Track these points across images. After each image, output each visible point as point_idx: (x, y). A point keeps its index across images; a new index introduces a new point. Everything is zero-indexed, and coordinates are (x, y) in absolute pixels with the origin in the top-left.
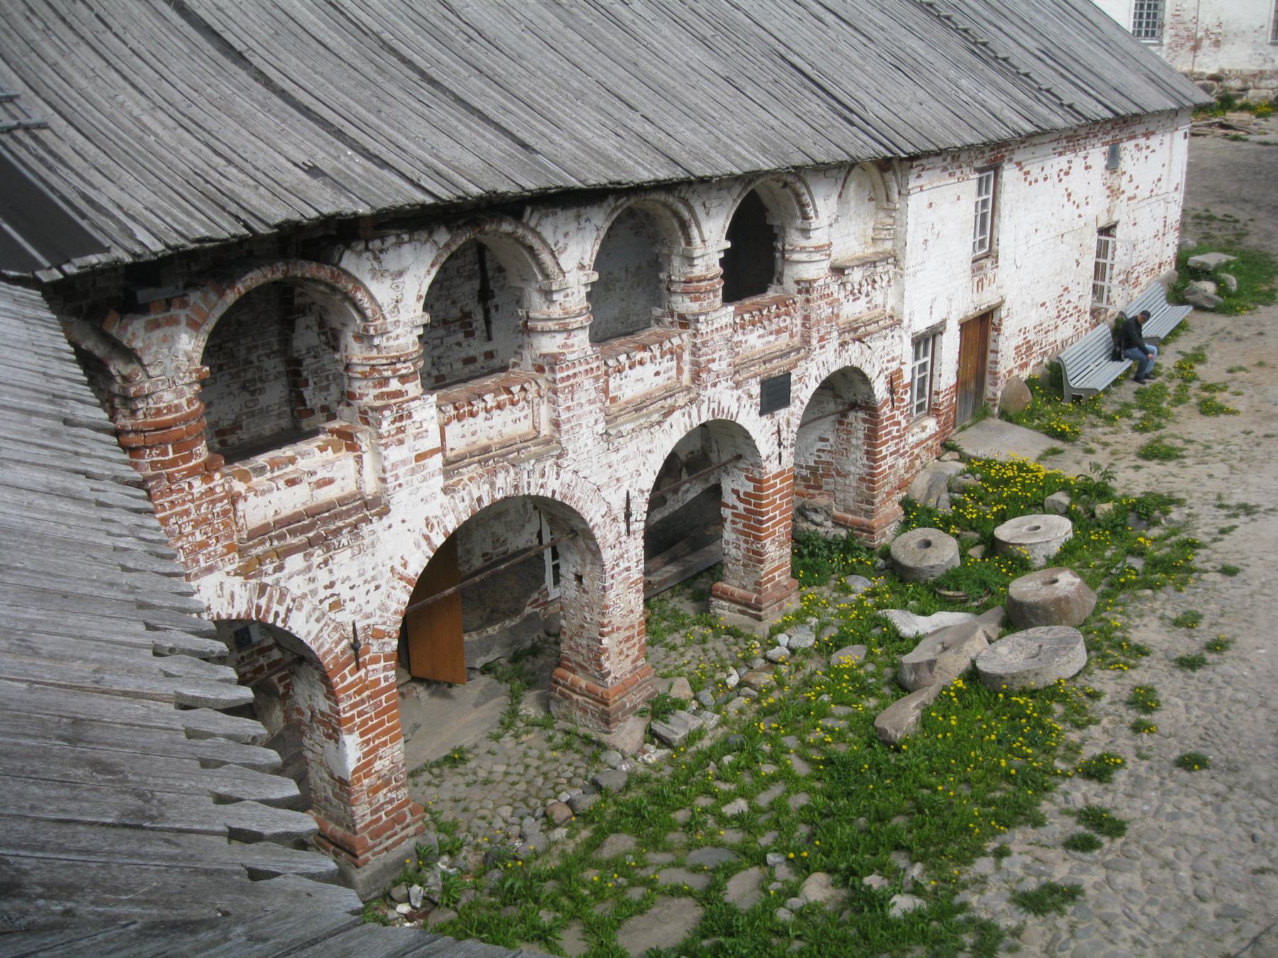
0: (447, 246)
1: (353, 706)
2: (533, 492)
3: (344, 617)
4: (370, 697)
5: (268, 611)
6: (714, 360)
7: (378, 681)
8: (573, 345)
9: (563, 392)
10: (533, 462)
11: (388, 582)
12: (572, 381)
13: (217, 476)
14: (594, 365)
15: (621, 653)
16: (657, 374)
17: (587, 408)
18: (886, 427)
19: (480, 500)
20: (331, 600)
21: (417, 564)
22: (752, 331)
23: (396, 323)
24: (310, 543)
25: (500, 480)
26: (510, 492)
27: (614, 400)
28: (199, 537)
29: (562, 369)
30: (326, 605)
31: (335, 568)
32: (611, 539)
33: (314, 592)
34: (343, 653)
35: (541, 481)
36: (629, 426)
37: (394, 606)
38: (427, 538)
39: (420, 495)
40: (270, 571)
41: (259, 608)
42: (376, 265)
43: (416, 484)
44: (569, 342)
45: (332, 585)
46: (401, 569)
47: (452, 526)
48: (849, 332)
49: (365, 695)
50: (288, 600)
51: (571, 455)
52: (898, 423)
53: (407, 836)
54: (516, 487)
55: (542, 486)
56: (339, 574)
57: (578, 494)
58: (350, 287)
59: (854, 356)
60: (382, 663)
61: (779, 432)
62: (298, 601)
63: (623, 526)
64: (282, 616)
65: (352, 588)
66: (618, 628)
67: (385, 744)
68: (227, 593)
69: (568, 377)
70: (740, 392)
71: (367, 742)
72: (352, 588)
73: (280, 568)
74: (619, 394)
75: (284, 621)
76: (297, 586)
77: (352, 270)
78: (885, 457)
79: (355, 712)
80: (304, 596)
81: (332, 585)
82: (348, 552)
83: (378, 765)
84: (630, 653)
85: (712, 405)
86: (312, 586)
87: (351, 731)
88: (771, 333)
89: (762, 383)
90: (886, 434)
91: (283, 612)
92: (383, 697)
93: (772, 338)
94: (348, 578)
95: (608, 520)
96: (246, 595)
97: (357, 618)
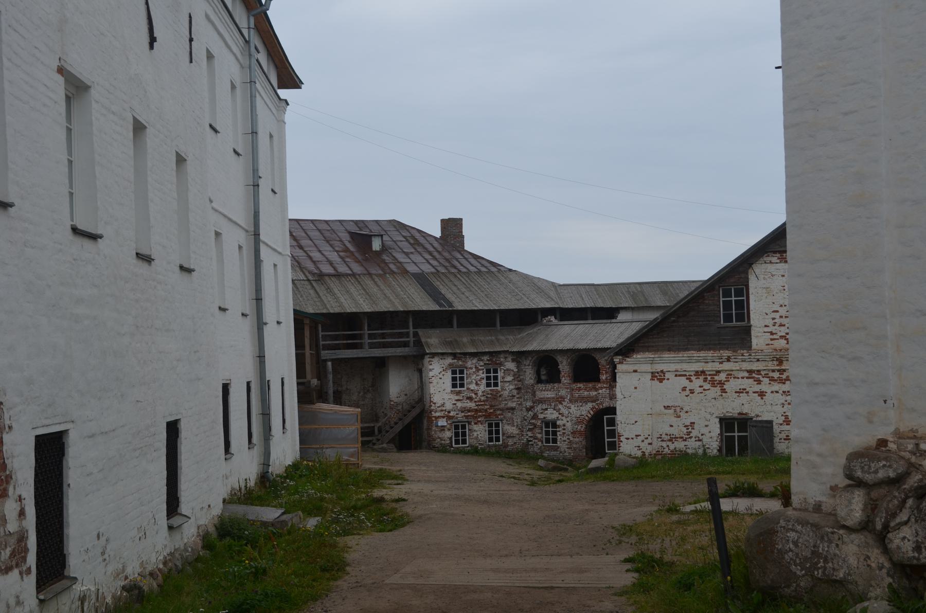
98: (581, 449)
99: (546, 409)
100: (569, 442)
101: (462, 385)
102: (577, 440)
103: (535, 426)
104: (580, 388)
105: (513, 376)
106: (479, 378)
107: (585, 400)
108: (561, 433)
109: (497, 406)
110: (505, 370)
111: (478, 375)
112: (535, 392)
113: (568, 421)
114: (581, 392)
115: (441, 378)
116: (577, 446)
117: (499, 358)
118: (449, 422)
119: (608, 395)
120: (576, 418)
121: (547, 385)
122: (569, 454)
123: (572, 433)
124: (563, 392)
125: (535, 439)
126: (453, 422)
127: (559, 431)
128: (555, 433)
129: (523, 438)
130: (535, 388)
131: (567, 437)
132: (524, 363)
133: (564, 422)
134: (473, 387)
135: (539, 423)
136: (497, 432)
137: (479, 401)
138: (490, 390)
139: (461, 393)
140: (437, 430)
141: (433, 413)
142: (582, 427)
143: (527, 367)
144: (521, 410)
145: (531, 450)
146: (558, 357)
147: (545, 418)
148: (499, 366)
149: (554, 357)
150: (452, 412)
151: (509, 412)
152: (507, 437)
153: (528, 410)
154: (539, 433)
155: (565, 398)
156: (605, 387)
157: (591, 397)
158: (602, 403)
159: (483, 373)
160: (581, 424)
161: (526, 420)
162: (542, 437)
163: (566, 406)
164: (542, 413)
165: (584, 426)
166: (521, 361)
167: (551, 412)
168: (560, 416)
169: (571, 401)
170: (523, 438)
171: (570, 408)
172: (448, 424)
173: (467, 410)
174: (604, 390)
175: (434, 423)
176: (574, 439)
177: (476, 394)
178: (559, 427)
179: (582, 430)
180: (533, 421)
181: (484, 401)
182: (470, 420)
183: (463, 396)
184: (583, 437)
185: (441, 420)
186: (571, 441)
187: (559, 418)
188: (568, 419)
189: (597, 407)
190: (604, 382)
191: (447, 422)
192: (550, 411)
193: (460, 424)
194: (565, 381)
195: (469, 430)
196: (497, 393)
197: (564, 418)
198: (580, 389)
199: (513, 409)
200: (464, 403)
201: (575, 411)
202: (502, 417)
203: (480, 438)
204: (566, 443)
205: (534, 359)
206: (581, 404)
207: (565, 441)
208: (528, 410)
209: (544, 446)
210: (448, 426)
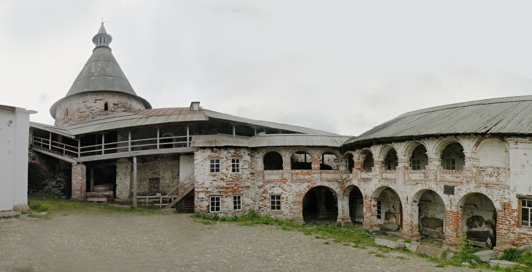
0: (381, 147)
3: (365, 192)
6: (430, 176)
12: (399, 171)
16: (420, 176)
18: (502, 219)
22: (448, 175)
26: (387, 185)
27: (410, 178)
45: (365, 187)
48: (484, 184)
52: (510, 221)
53: (367, 227)
56: (366, 186)
59: (483, 190)
61: (451, 200)
70: (437, 186)
76: (362, 185)
78: (502, 229)
81: (365, 187)
83: (367, 215)
85: (429, 186)
88: (454, 177)
89: (444, 186)
90: (501, 221)
93: (455, 178)
98: (299, 213)
99: (274, 187)
100: (290, 209)
101: (218, 170)
102: (296, 207)
105: (249, 165)
106: (228, 165)
107: (303, 181)
109: (239, 185)
110: (244, 161)
111: (228, 163)
112: (264, 176)
113: (290, 195)
115: (202, 165)
116: (297, 211)
117: (240, 152)
118: (207, 196)
119: (319, 178)
122: (290, 216)
124: (286, 176)
126: (210, 196)
127: (283, 201)
128: (279, 203)
130: (264, 173)
132: (257, 156)
133: (287, 195)
134: (224, 171)
135: (268, 196)
136: (239, 202)
137: (228, 182)
138: (235, 174)
139: (216, 176)
140: (198, 200)
141: (195, 189)
143: (258, 159)
144: (255, 188)
145: (262, 214)
146: (283, 152)
147: (272, 193)
148: (240, 157)
149: (279, 152)
150: (209, 189)
151: (246, 189)
152: (246, 206)
153: (260, 187)
154: (268, 203)
155: (287, 180)
156: (317, 173)
157: (306, 179)
158: (315, 183)
159: (231, 162)
160: (300, 197)
161: (258, 194)
162: (270, 205)
164: (270, 189)
165: (302, 198)
166: (253, 155)
169: (292, 182)
170: (255, 206)
171: (292, 186)
172: (206, 197)
173: (220, 187)
175: (196, 196)
176: (294, 206)
177: (226, 176)
179: (300, 201)
180: (264, 195)
181: (231, 181)
182: (222, 194)
183: (218, 178)
184: (301, 205)
185: (200, 193)
187: (283, 193)
188: (290, 194)
189: (311, 186)
190: (316, 169)
191: (205, 195)
192: (276, 188)
193: (215, 197)
194: (288, 169)
195: (222, 201)
196: (240, 176)
197: (287, 193)
198: (297, 174)
199: (248, 187)
200: (218, 182)
201: (295, 188)
202: (242, 192)
203: (229, 207)
204: (289, 209)
205: (264, 153)
206: (299, 183)
207: (287, 208)
208: (260, 187)
209: (271, 211)
210: (206, 198)
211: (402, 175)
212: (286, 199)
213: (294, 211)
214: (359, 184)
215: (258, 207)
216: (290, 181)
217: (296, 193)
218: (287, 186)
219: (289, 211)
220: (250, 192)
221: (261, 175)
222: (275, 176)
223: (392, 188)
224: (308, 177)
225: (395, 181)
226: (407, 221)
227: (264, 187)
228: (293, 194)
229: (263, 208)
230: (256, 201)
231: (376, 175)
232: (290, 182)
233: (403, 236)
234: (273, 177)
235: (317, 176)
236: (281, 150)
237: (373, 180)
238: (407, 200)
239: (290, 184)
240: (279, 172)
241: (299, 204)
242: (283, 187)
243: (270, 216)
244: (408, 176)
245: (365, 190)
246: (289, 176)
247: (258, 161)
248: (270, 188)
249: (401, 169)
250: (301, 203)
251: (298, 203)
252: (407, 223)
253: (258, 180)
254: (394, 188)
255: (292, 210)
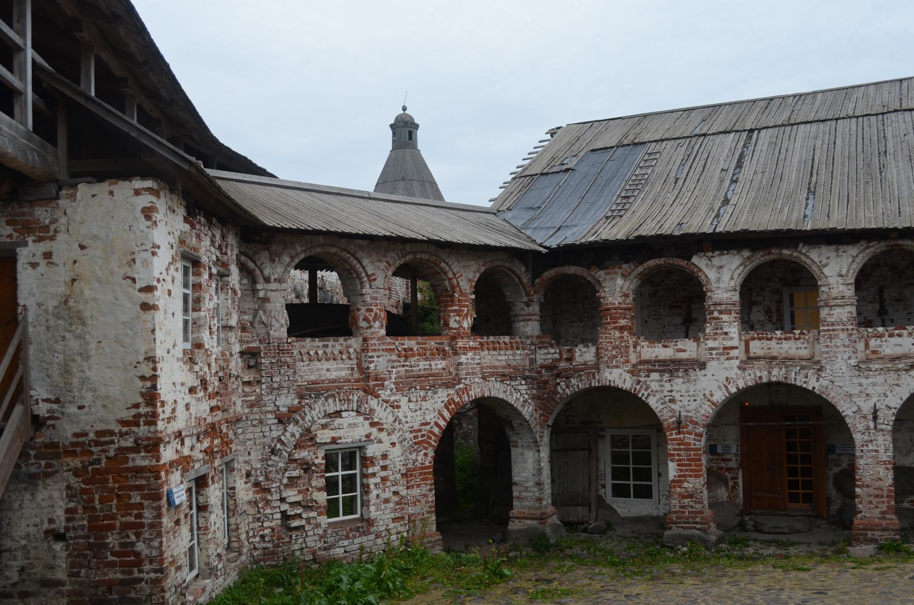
1: (675, 449)
2: (798, 383)
4: (684, 449)
5: (639, 391)
7: (689, 444)
8: (833, 314)
9: (823, 337)
10: (798, 368)
11: (701, 400)
12: (831, 333)
13: (626, 332)
14: (850, 327)
15: (870, 502)
17: (842, 349)
19: (761, 378)
20: (670, 398)
21: (719, 396)
23: (718, 288)
24: (664, 371)
25: (775, 372)
26: (781, 379)
27: (874, 352)
28: (614, 353)
29: (823, 325)
30: (667, 399)
31: (674, 385)
32: (860, 427)
33: (662, 391)
34: (673, 423)
35: (804, 380)
36: (877, 366)
37: (703, 412)
38: (726, 387)
39: (724, 365)
40: (643, 376)
41: (635, 389)
42: (709, 262)
43: (722, 360)
44: (831, 312)
45: (671, 391)
46: (709, 397)
47: (741, 385)
49: (682, 447)
50: (649, 390)
51: (828, 371)
53: (695, 528)
54: (786, 378)
55: (805, 382)
56: (675, 387)
57: (832, 394)
58: (695, 270)
60: (693, 436)
62: (654, 393)
63: (872, 424)
64: (645, 396)
65: (681, 396)
66: (868, 486)
67: (691, 476)
68: (623, 378)
69: (828, 330)
71: (681, 471)
72: (681, 396)
73: (648, 376)
74: (880, 349)
75: (646, 398)
76: (654, 386)
77: (696, 263)
79: (676, 452)
80: (657, 391)
82: (682, 380)
83: (686, 485)
84: (880, 506)
86: (661, 388)
87: (672, 461)
91: (646, 394)
92: (692, 453)
94: (680, 391)
95: (858, 416)
96: (631, 382)
97: (682, 410)
98: (426, 515)
99: (338, 414)
100: (397, 503)
102: (416, 492)
103: (307, 467)
104: (411, 349)
108: (378, 480)
113: (393, 444)
114: (412, 360)
120: (411, 432)
121: (330, 344)
123: (404, 475)
125: (307, 508)
129: (268, 511)
131: (393, 489)
133: (385, 447)
142: (426, 455)
143: (273, 286)
144: (261, 422)
147: (334, 441)
155: (384, 379)
156: (471, 349)
158: (466, 389)
160: (426, 448)
163: (386, 402)
164: (324, 426)
165: (431, 453)
167: (350, 421)
168: (374, 430)
171: (399, 407)
174: (470, 354)
178: (373, 464)
179: (427, 464)
180: (303, 454)
184: (429, 482)
186: (402, 498)
187: (372, 437)
188: (394, 438)
189: (457, 400)
197: (383, 436)
201: (409, 414)
204: (391, 505)
206: (422, 393)
207: (387, 501)
208: (283, 420)
211: (847, 343)
212: (382, 463)
213: (411, 510)
214: (639, 382)
215: (279, 516)
216: (393, 386)
217: (412, 436)
218: (382, 406)
219: (392, 516)
220: (244, 443)
221: (288, 359)
222: (332, 365)
223: (804, 386)
224: (440, 366)
225: (814, 364)
226: (877, 484)
227: (303, 419)
228: (405, 439)
229: (299, 516)
230: (268, 491)
231: (725, 348)
232: (391, 390)
233: (866, 534)
234: (328, 370)
235: (472, 359)
236: (359, 254)
237: (712, 366)
238: (875, 418)
239: (392, 399)
240: (350, 347)
241: (423, 479)
242: (371, 410)
243: (331, 547)
244: (867, 346)
245: (672, 401)
246: (390, 364)
247: (271, 295)
248: (324, 421)
249: (840, 327)
250: (429, 473)
251: (421, 474)
252: (877, 489)
253: (275, 385)
254: (817, 385)
255: (403, 509)
